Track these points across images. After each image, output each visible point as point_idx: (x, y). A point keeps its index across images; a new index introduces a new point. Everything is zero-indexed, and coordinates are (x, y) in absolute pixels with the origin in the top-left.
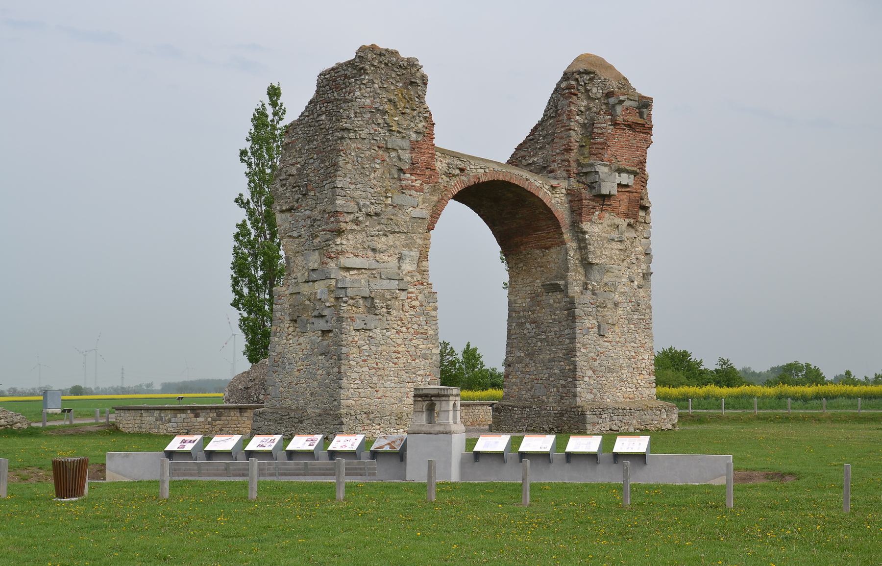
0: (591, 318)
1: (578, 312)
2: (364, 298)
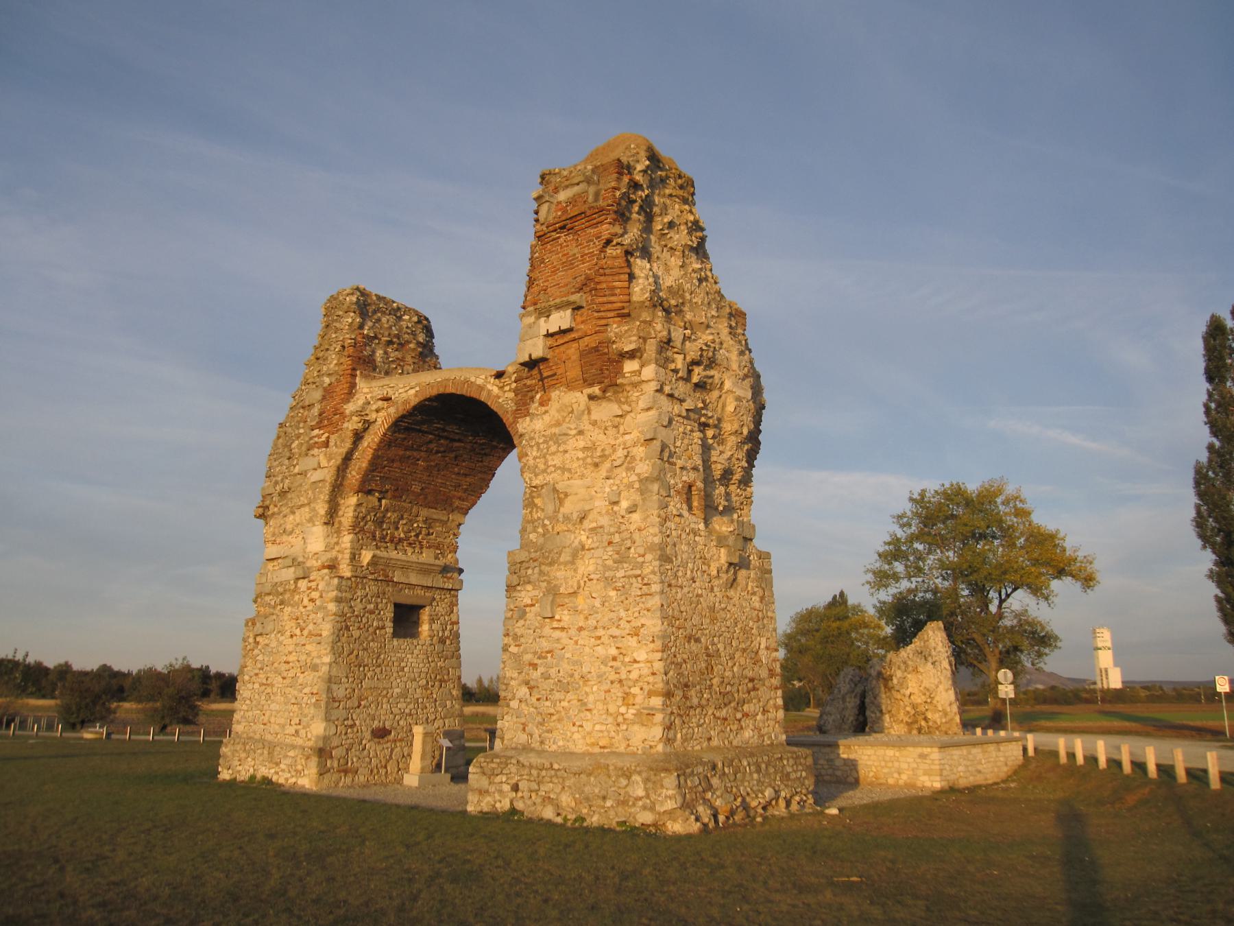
0: (529, 587)
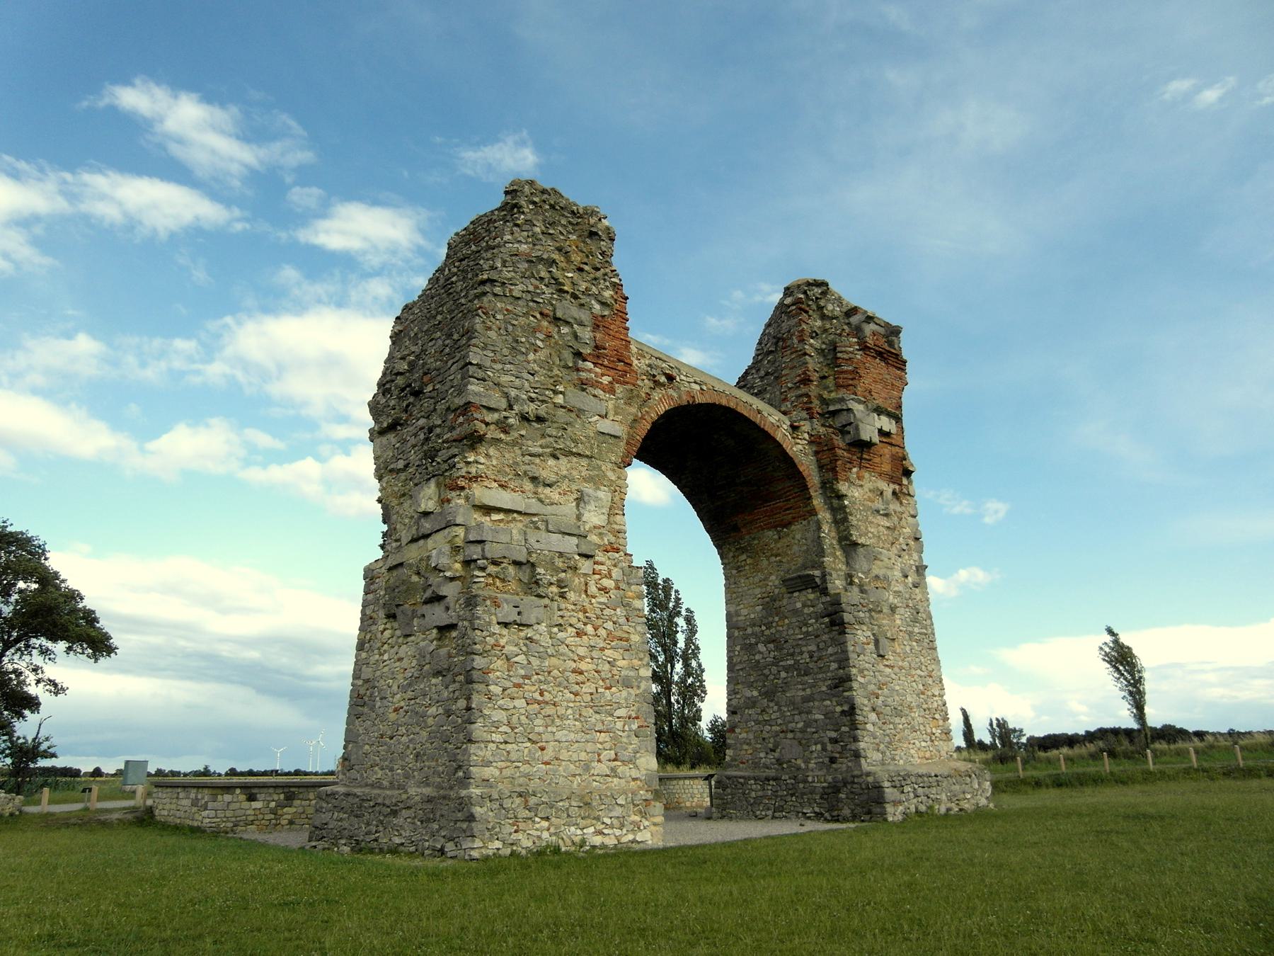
0: (865, 628)
1: (847, 617)
2: (517, 563)
